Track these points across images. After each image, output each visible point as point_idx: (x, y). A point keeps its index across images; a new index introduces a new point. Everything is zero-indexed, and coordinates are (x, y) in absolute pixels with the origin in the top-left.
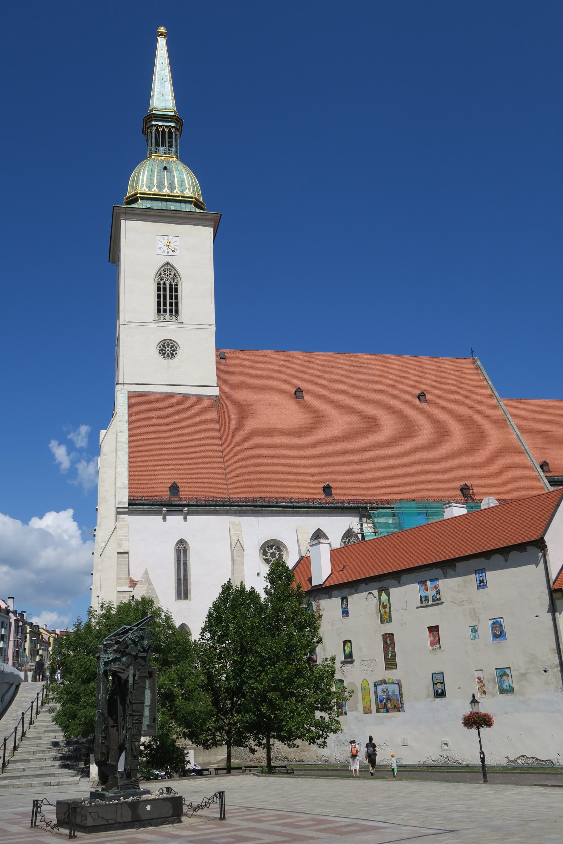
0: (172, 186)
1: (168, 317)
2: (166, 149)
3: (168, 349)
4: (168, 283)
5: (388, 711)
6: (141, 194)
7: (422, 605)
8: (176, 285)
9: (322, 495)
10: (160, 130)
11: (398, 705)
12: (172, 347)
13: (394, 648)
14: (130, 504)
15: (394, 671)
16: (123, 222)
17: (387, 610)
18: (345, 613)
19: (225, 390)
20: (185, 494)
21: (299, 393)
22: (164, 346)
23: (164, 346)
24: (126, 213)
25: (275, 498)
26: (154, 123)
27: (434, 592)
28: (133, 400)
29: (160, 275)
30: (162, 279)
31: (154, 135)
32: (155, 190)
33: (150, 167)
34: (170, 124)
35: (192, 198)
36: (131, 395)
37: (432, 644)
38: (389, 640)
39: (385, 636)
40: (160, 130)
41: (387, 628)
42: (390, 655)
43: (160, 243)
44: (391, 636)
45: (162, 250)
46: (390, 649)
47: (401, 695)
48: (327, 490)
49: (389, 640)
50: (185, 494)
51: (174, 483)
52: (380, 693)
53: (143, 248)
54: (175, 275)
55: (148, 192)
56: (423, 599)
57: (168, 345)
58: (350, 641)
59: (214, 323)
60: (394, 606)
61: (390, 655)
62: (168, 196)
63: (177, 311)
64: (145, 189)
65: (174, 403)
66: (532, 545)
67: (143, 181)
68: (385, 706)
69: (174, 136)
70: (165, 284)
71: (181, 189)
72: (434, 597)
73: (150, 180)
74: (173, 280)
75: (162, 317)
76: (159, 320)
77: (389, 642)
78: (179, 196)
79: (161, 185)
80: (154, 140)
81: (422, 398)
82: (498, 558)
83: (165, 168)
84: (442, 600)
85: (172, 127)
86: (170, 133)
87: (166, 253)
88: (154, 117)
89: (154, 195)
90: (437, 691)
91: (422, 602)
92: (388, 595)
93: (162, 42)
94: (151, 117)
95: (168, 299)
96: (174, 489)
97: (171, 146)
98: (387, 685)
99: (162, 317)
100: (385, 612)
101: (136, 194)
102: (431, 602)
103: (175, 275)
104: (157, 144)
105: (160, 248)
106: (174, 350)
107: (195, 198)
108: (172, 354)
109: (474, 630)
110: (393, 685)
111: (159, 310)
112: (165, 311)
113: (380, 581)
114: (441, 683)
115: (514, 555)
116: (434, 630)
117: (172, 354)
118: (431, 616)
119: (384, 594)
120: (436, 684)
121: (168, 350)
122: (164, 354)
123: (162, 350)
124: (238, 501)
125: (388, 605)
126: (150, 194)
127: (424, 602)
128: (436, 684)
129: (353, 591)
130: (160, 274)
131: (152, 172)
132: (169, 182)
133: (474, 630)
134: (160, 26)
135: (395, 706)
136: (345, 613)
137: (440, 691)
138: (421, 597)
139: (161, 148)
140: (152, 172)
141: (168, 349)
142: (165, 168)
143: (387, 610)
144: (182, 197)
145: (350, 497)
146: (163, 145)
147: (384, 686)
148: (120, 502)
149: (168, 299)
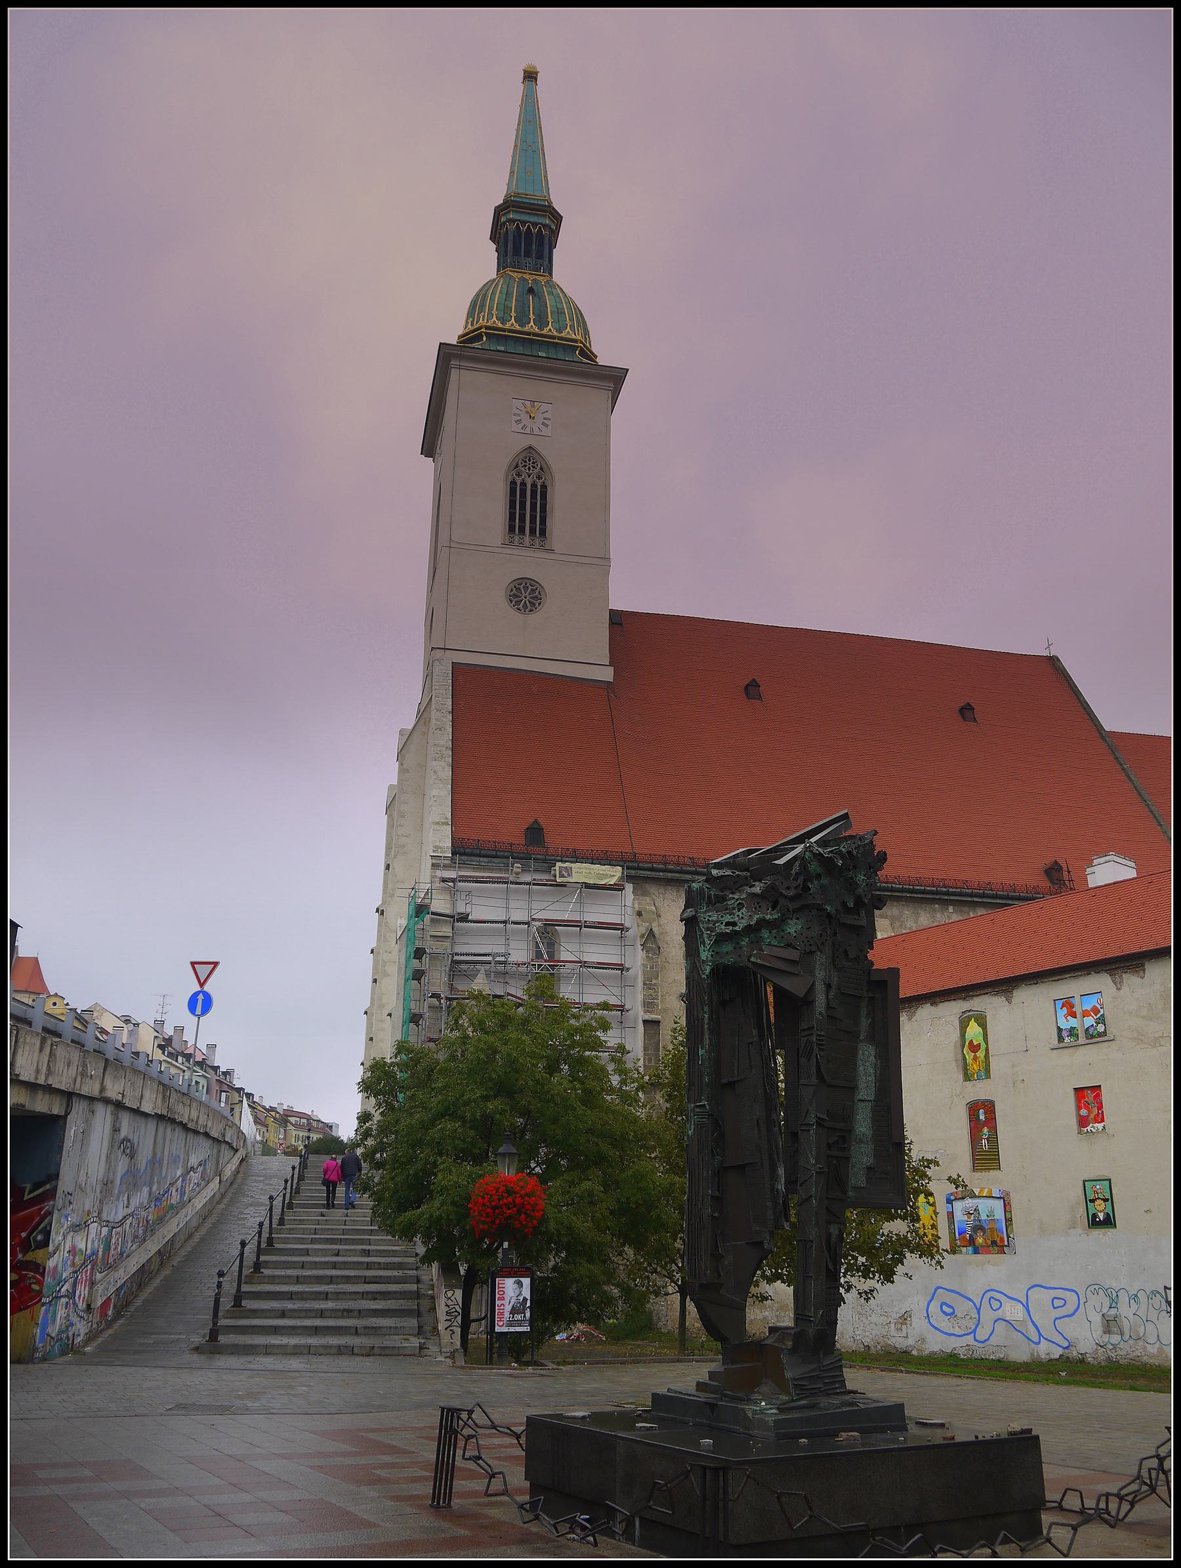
0: (541, 321)
1: (527, 539)
4: (529, 482)
5: (976, 1252)
6: (487, 328)
7: (1061, 1045)
8: (544, 487)
10: (524, 229)
11: (1002, 1240)
13: (994, 1129)
15: (993, 1173)
16: (454, 374)
17: (981, 1054)
30: (519, 475)
31: (510, 238)
32: (512, 324)
33: (505, 287)
35: (576, 341)
37: (1083, 1122)
39: (973, 1108)
40: (524, 229)
41: (979, 1091)
43: (518, 412)
44: (989, 1107)
45: (521, 425)
46: (986, 1130)
47: (1009, 1221)
52: (959, 1216)
55: (500, 325)
56: (1065, 1034)
62: (535, 335)
63: (543, 532)
64: (494, 321)
67: (491, 308)
68: (971, 1242)
69: (546, 241)
70: (523, 484)
72: (1091, 1031)
74: (539, 478)
75: (516, 538)
77: (982, 1117)
78: (554, 337)
79: (522, 319)
80: (510, 246)
83: (531, 291)
84: (1110, 1036)
85: (545, 226)
87: (528, 430)
88: (514, 206)
89: (510, 331)
90: (1095, 1216)
91: (1061, 1039)
92: (983, 1024)
98: (976, 1201)
99: (516, 538)
100: (975, 1058)
101: (480, 328)
102: (1082, 1040)
103: (541, 469)
104: (516, 252)
108: (533, 604)
110: (991, 1202)
111: (511, 529)
113: (964, 999)
114: (1105, 1200)
118: (1086, 1065)
119: (973, 1023)
120: (1092, 1201)
121: (526, 596)
122: (518, 603)
125: (983, 1046)
126: (504, 330)
127: (1067, 1040)
128: (1092, 1201)
130: (517, 466)
131: (508, 295)
135: (994, 1243)
137: (1101, 1216)
138: (1060, 1030)
143: (981, 1054)
144: (560, 338)
147: (969, 1202)
148: (437, 847)
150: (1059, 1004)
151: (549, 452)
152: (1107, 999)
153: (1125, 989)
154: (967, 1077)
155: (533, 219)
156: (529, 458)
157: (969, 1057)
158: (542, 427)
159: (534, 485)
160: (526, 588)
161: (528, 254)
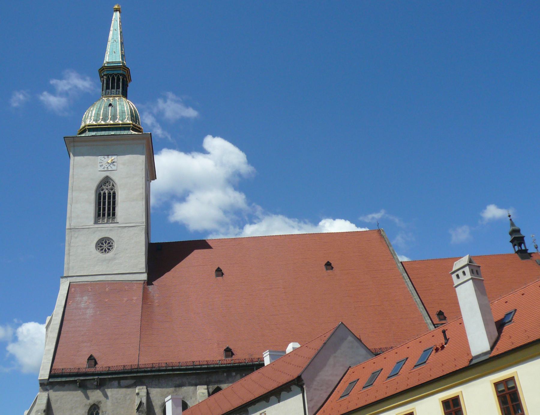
0: (114, 117)
2: (114, 91)
3: (105, 245)
4: (107, 192)
6: (89, 126)
8: (114, 193)
12: (109, 243)
24: (74, 142)
25: (179, 363)
28: (73, 290)
29: (100, 187)
35: (130, 124)
43: (101, 161)
54: (113, 185)
63: (114, 214)
65: (107, 289)
66: (295, 384)
67: (91, 116)
70: (104, 193)
71: (121, 119)
73: (98, 115)
74: (112, 189)
78: (119, 124)
79: (105, 118)
82: (273, 398)
83: (110, 105)
87: (106, 169)
93: (116, 16)
94: (104, 69)
95: (106, 204)
101: (86, 126)
104: (108, 88)
105: (101, 166)
106: (110, 246)
107: (133, 125)
111: (99, 215)
112: (104, 215)
115: (283, 394)
121: (105, 246)
132: (113, 114)
140: (100, 109)
141: (105, 245)
142: (110, 105)
144: (122, 124)
149: (106, 204)
151: (114, 177)
155: (115, 72)
156: (106, 180)
159: (109, 193)
160: (106, 242)
161: (113, 88)
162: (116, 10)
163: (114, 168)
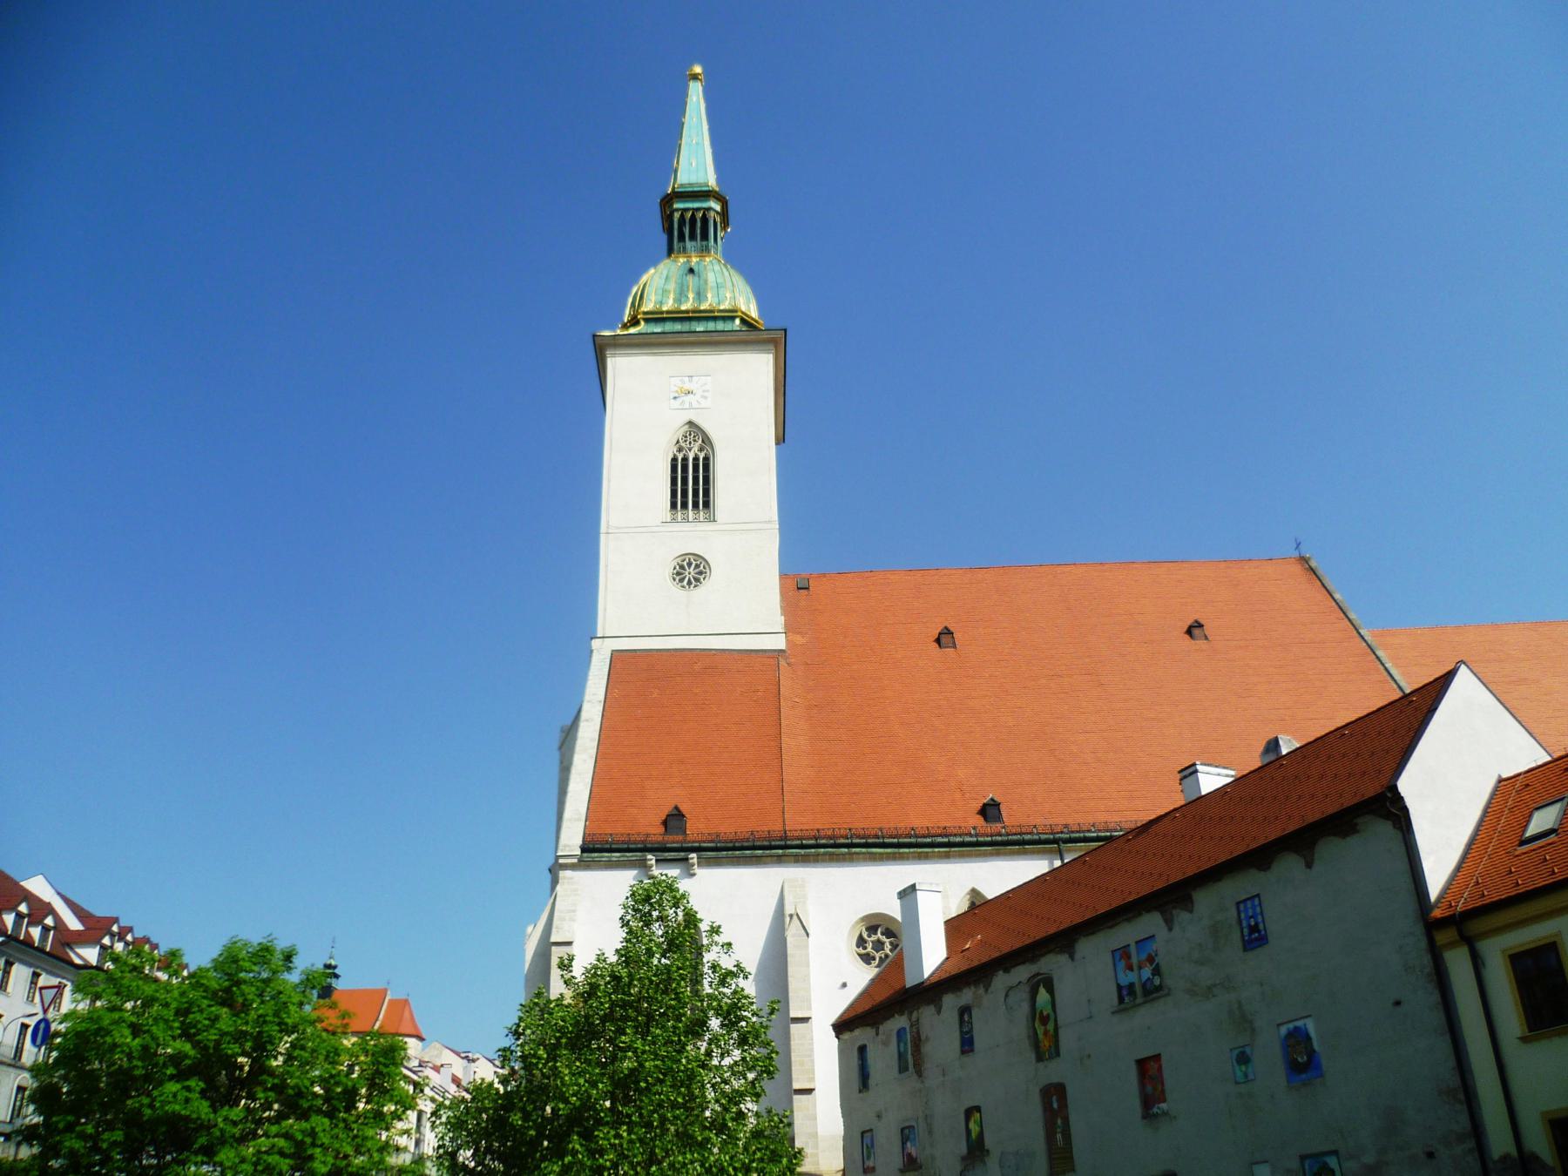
0: (700, 296)
3: (691, 571)
8: (706, 459)
9: (979, 821)
12: (697, 566)
13: (1066, 1120)
14: (584, 849)
17: (1051, 1026)
18: (967, 1045)
19: (799, 639)
20: (696, 828)
21: (944, 638)
22: (682, 567)
23: (682, 567)
26: (676, 206)
27: (1147, 972)
34: (705, 205)
36: (618, 657)
38: (1054, 1098)
41: (1053, 1072)
42: (1059, 1136)
48: (990, 811)
49: (1054, 1098)
50: (696, 828)
51: (676, 808)
53: (647, 399)
57: (690, 564)
58: (978, 1109)
59: (776, 518)
60: (1064, 1016)
61: (1059, 1136)
63: (706, 505)
70: (685, 459)
76: (674, 520)
79: (681, 295)
81: (1196, 632)
86: (705, 220)
91: (1121, 1000)
95: (692, 484)
96: (675, 819)
97: (705, 237)
100: (1046, 1033)
106: (701, 573)
109: (1243, 1059)
111: (673, 505)
112: (685, 505)
116: (1148, 1068)
117: (697, 580)
121: (691, 572)
122: (681, 580)
123: (678, 574)
124: (801, 839)
127: (1127, 999)
129: (981, 991)
133: (1243, 1059)
134: (691, 65)
136: (967, 1045)
138: (1120, 988)
139: (689, 244)
142: (691, 271)
143: (1051, 1026)
145: (1039, 821)
146: (693, 237)
149: (692, 484)
150: (1117, 955)
152: (1158, 945)
153: (1176, 928)
154: (1040, 1058)
155: (696, 205)
157: (1040, 1030)
158: (703, 401)
159: (696, 459)
162: (695, 77)
163: (704, 403)
